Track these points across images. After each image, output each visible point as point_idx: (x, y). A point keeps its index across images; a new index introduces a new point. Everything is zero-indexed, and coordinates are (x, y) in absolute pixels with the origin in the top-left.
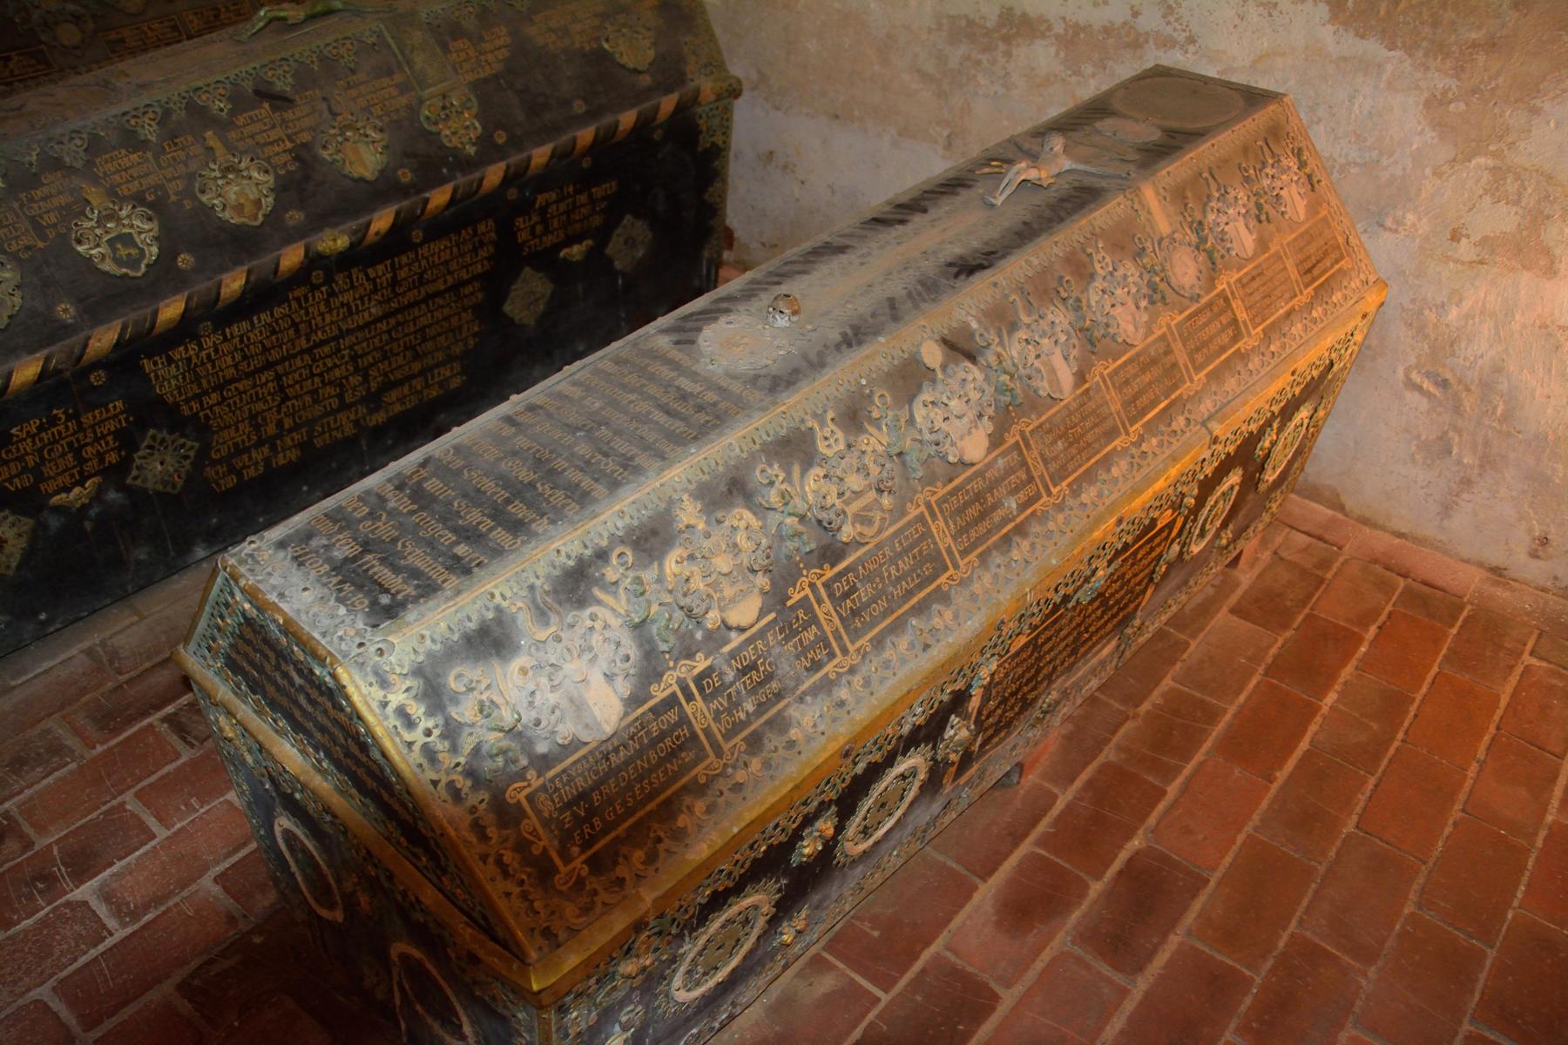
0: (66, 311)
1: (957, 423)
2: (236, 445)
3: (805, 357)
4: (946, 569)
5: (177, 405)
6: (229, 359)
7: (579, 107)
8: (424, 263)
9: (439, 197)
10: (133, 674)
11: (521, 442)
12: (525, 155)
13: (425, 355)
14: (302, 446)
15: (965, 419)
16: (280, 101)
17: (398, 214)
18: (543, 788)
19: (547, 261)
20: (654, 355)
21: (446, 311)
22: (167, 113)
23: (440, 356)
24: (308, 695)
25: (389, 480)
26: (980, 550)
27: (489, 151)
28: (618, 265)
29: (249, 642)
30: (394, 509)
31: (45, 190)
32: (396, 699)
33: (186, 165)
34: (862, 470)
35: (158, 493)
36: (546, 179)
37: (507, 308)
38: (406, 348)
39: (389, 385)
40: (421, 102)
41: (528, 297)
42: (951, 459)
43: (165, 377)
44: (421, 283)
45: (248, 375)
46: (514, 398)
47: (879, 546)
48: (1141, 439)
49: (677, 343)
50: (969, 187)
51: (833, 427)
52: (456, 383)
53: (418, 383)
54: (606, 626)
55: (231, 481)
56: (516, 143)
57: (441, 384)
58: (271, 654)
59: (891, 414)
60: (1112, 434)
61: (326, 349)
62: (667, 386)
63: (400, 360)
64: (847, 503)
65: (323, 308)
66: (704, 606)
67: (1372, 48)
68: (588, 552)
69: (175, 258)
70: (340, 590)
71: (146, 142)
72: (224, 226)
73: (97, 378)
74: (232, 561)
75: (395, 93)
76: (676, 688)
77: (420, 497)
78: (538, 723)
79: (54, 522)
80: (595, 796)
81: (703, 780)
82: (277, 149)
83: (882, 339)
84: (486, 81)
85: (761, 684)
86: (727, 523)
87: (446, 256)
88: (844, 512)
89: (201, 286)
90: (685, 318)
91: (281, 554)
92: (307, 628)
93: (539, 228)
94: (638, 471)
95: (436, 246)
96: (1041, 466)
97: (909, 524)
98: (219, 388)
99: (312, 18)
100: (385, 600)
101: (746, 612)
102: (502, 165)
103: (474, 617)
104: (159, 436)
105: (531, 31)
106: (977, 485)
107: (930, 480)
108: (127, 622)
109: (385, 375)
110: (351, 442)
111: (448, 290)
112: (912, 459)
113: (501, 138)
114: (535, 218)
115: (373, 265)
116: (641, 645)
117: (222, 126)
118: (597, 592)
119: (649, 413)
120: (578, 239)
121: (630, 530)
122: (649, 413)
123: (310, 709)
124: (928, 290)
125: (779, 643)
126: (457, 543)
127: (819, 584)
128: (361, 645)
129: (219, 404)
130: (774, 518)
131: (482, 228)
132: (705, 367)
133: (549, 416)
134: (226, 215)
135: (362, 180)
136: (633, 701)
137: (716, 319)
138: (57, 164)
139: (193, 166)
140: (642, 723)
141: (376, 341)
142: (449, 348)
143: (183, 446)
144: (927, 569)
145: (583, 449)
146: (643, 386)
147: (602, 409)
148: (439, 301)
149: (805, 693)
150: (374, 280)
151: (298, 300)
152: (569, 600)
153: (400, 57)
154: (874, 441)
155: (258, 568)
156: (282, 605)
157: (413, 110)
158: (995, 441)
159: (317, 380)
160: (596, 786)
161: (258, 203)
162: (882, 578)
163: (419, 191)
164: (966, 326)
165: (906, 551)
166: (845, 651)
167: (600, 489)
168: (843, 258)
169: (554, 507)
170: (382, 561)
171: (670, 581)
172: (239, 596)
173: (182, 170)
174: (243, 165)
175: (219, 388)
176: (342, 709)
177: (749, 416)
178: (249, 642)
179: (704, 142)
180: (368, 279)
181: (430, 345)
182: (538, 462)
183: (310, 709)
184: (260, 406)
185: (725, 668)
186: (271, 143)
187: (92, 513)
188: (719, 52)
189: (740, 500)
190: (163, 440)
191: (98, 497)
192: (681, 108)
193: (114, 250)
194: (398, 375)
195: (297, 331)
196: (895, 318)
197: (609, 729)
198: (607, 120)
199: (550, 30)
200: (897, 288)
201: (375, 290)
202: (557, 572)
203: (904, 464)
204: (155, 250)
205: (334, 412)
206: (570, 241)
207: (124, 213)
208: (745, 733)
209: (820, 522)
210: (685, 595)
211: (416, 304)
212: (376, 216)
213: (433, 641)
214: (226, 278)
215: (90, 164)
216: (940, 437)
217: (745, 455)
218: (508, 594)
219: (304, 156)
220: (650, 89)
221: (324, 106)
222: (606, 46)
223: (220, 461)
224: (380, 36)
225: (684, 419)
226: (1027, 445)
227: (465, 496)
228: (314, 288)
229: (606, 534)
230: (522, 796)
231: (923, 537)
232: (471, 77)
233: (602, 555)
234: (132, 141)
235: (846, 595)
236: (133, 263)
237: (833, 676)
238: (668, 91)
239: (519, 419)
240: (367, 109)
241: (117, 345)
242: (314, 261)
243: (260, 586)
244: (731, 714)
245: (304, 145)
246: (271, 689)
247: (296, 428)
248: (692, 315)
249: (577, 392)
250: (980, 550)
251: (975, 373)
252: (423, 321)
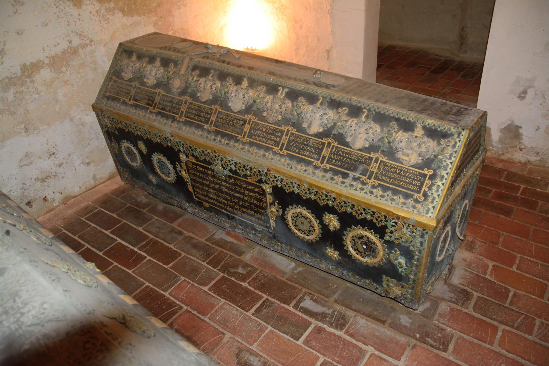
67: (136, 18)
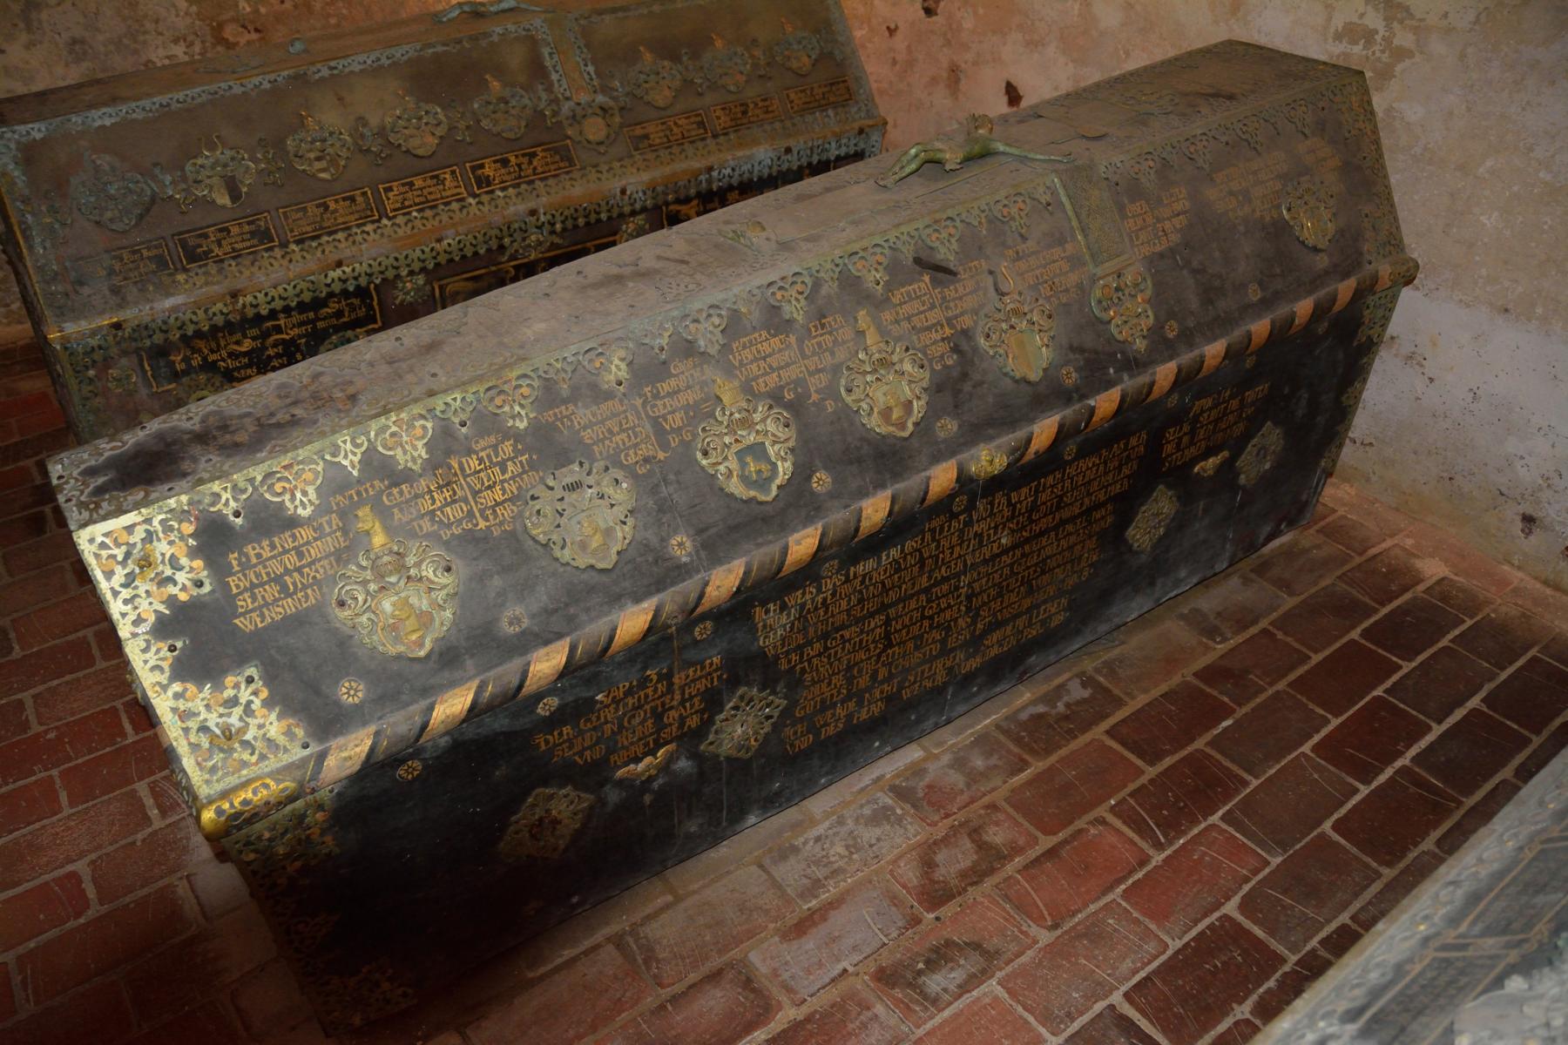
0: (681, 546)
6: (844, 604)
7: (1254, 293)
9: (1106, 403)
10: (678, 988)
12: (1196, 352)
13: (1039, 588)
14: (889, 699)
16: (941, 272)
19: (1181, 479)
22: (817, 284)
27: (1162, 347)
28: (1242, 479)
31: (673, 382)
33: (833, 354)
35: (728, 758)
37: (1130, 532)
40: (1094, 280)
44: (1059, 508)
45: (858, 621)
53: (1020, 622)
56: (1188, 337)
57: (1043, 622)
61: (945, 587)
63: (1013, 598)
65: (955, 539)
69: (810, 477)
71: (790, 322)
72: (869, 438)
75: (1066, 267)
79: (613, 796)
82: (935, 336)
84: (1161, 255)
89: (838, 517)
93: (1185, 439)
98: (825, 636)
105: (1211, 194)
110: (940, 691)
111: (1081, 515)
115: (1018, 488)
117: (878, 304)
129: (820, 655)
131: (1133, 441)
138: (687, 349)
139: (841, 355)
141: (997, 576)
148: (1070, 528)
151: (933, 531)
153: (1075, 223)
161: (908, 405)
163: (1083, 397)
173: (828, 360)
180: (1009, 503)
184: (862, 655)
186: (928, 329)
187: (655, 785)
188: (1398, 228)
191: (665, 768)
193: (743, 465)
195: (922, 567)
198: (1282, 311)
199: (1231, 193)
211: (1042, 534)
215: (726, 348)
220: (1327, 272)
221: (990, 280)
224: (1054, 193)
228: (954, 516)
232: (1146, 250)
234: (775, 321)
238: (1346, 275)
245: (966, 334)
247: (888, 679)
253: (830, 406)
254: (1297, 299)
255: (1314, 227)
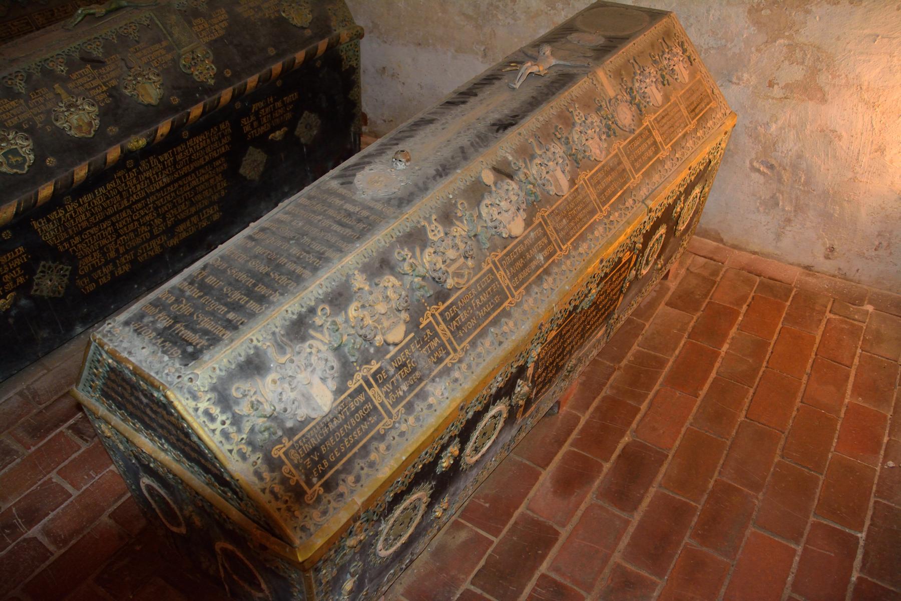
1: (506, 215)
2: (93, 266)
3: (416, 185)
4: (508, 298)
5: (56, 245)
7: (272, 51)
8: (191, 150)
9: (196, 111)
10: (48, 403)
11: (258, 250)
12: (243, 82)
14: (131, 262)
15: (510, 212)
16: (97, 63)
17: (173, 123)
18: (293, 446)
19: (261, 142)
20: (332, 193)
21: (207, 177)
22: (30, 76)
23: (206, 203)
24: (151, 409)
25: (185, 280)
26: (525, 285)
27: (222, 82)
28: (303, 140)
29: (114, 381)
30: (190, 296)
32: (203, 405)
33: (45, 105)
34: (455, 246)
35: (50, 298)
36: (257, 94)
37: (242, 171)
38: (186, 200)
39: (177, 223)
40: (180, 57)
41: (253, 164)
42: (504, 235)
43: (46, 231)
45: (95, 225)
46: (252, 225)
47: (468, 289)
48: (609, 214)
49: (342, 184)
50: (499, 79)
51: (436, 224)
52: (216, 217)
53: (194, 219)
54: (319, 351)
55: (92, 287)
56: (237, 75)
57: (208, 218)
58: (128, 387)
59: (468, 213)
60: (593, 212)
61: (140, 205)
62: (339, 209)
63: (183, 206)
64: (448, 266)
65: (135, 181)
66: (373, 334)
68: (304, 310)
69: (45, 161)
70: (163, 346)
73: (7, 235)
74: (99, 336)
75: (163, 52)
76: (362, 382)
77: (204, 287)
78: (285, 410)
80: (323, 448)
81: (382, 432)
83: (459, 171)
84: (216, 41)
85: (410, 374)
86: (381, 285)
87: (203, 144)
88: (447, 272)
89: (62, 176)
90: (346, 169)
91: (127, 329)
92: (147, 370)
93: (255, 124)
94: (328, 260)
95: (197, 140)
96: (555, 235)
97: (484, 275)
98: (79, 233)
99: (109, 12)
100: (190, 349)
101: (397, 334)
102: (231, 89)
103: (243, 354)
104: (47, 265)
105: (239, 10)
106: (520, 249)
107: (493, 248)
108: (40, 374)
109: (176, 216)
111: (205, 165)
112: (483, 238)
113: (228, 73)
114: (252, 118)
115: (161, 154)
116: (339, 360)
117: (64, 80)
118: (311, 332)
119: (330, 226)
120: (278, 128)
121: (327, 294)
122: (330, 226)
123: (153, 416)
124: (482, 141)
125: (418, 350)
126: (228, 312)
127: (437, 314)
128: (179, 377)
129: (80, 243)
130: (408, 279)
131: (222, 126)
132: (359, 197)
133: (273, 233)
134: (72, 133)
135: (150, 105)
136: (338, 392)
137: (364, 168)
139: (49, 105)
140: (345, 404)
141: (168, 197)
142: (210, 197)
143: (62, 269)
144: (497, 299)
145: (295, 251)
146: (325, 211)
147: (303, 226)
148: (203, 171)
149: (435, 377)
150: (163, 162)
151: (120, 178)
152: (296, 338)
153: (165, 32)
154: (460, 230)
155: (114, 339)
156: (131, 359)
157: (175, 62)
158: (528, 223)
159: (136, 223)
160: (323, 442)
161: (90, 124)
162: (472, 307)
163: (184, 109)
164: (506, 159)
165: (484, 290)
166: (455, 350)
167: (307, 273)
168: (432, 127)
169: (282, 285)
170: (186, 327)
171: (353, 322)
172: (105, 356)
174: (79, 103)
175: (79, 233)
176: (172, 414)
177: (387, 222)
178: (114, 381)
179: (345, 66)
180: (160, 162)
181: (199, 197)
182: (270, 261)
183: (153, 416)
184: (104, 241)
185: (389, 367)
186: (94, 88)
187: (13, 313)
188: (349, 13)
189: (387, 271)
190: (50, 267)
191: (14, 304)
192: (331, 47)
193: (8, 159)
194: (183, 216)
195: (121, 196)
196: (465, 158)
197: (326, 409)
198: (288, 58)
200: (464, 141)
201: (164, 168)
202: (287, 323)
203: (478, 241)
204: (32, 157)
205: (148, 241)
206: (273, 130)
207: (11, 137)
208: (404, 402)
209: (434, 279)
210: (362, 328)
212: (160, 125)
213: (221, 370)
214: (76, 169)
216: (497, 223)
217: (388, 245)
218: (261, 338)
219: (114, 93)
221: (123, 64)
222: (284, 15)
223: (84, 276)
224: (151, 20)
225: (351, 227)
226: (546, 223)
227: (230, 284)
228: (129, 170)
229: (313, 298)
230: (281, 453)
231: (493, 281)
232: (207, 40)
233: (312, 311)
235: (453, 319)
236: (20, 166)
237: (450, 365)
238: (322, 38)
239: (256, 237)
240: (148, 63)
241: (17, 214)
242: (127, 155)
243: (117, 349)
244: (394, 393)
245: (114, 88)
246: (130, 407)
247: (127, 252)
248: (349, 167)
249: (287, 218)
250: (525, 285)
251: (513, 185)
252: (194, 183)
253: (49, 129)
254: (296, 51)
255: (300, 17)
